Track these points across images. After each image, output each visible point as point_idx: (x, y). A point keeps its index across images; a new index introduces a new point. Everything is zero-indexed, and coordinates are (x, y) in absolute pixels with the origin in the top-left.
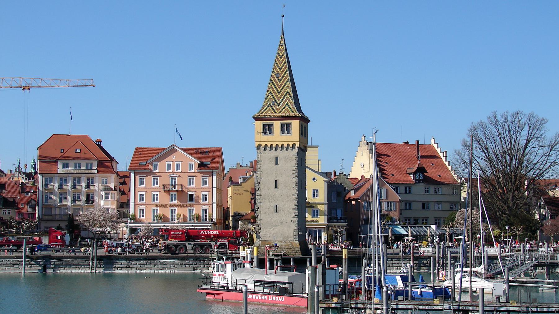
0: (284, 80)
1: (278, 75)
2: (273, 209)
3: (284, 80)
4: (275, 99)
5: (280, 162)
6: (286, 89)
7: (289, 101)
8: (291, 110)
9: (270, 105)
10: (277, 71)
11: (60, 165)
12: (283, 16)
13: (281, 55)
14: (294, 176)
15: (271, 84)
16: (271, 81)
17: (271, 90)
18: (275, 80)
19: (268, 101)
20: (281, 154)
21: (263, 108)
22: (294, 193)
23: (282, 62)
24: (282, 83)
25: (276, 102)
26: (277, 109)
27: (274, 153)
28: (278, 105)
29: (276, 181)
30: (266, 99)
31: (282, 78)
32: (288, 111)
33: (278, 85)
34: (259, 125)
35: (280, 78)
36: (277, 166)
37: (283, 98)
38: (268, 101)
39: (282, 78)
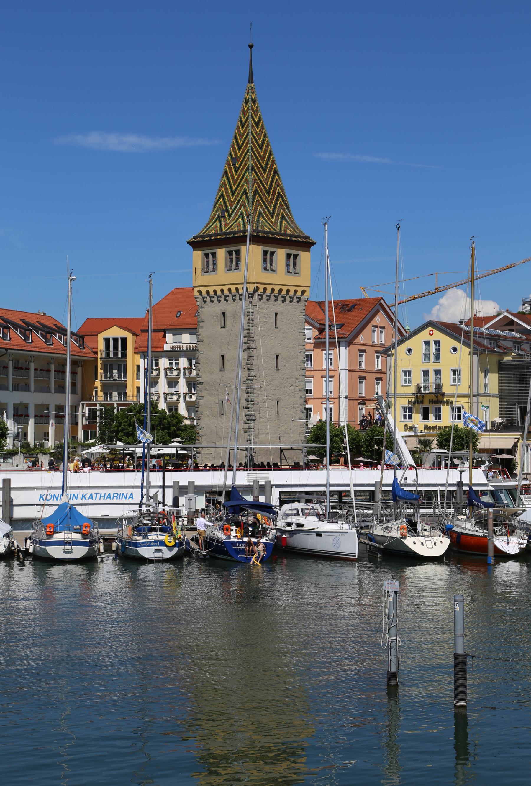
0: (243, 169)
1: (234, 160)
3: (243, 169)
6: (243, 186)
9: (218, 217)
10: (236, 154)
11: (169, 338)
12: (251, 47)
13: (244, 120)
14: (246, 346)
15: (225, 178)
16: (226, 173)
17: (223, 189)
19: (218, 210)
20: (230, 307)
21: (209, 224)
22: (245, 379)
25: (227, 210)
27: (217, 308)
28: (229, 216)
29: (223, 356)
30: (214, 208)
34: (198, 256)
35: (237, 166)
37: (238, 203)
38: (218, 210)
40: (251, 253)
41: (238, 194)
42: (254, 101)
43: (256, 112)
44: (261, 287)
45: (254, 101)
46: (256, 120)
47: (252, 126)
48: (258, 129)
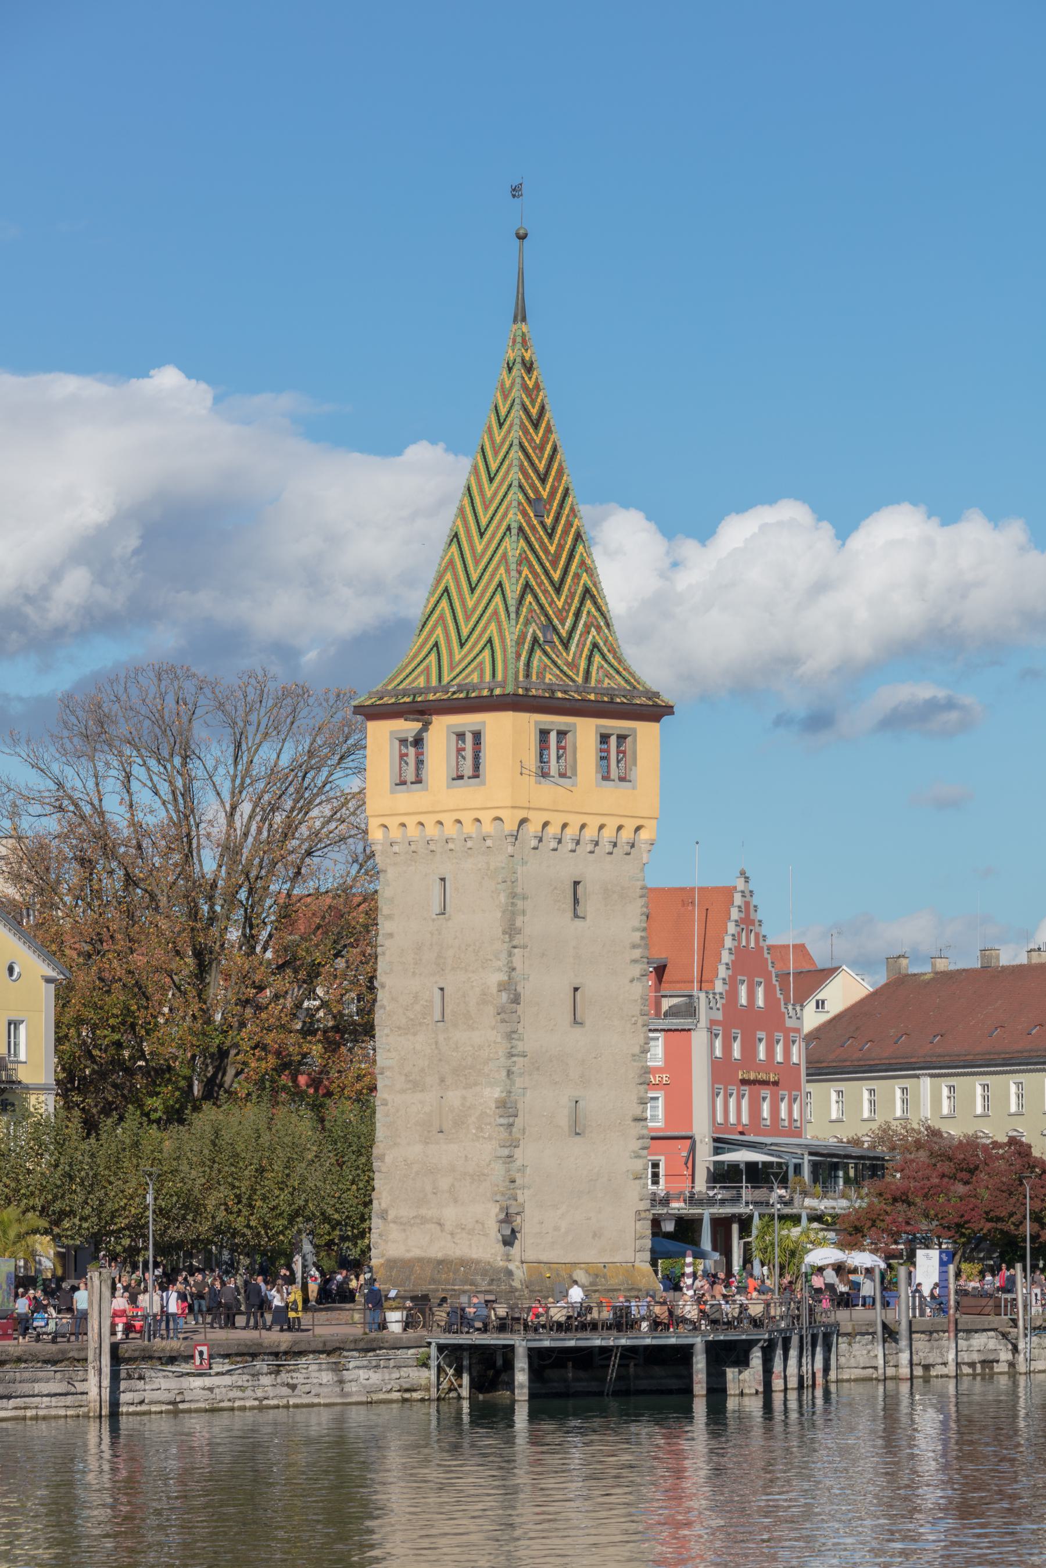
0: (566, 532)
2: (563, 1120)
4: (546, 615)
5: (590, 906)
6: (577, 576)
7: (599, 629)
8: (618, 672)
9: (535, 640)
10: (536, 491)
18: (533, 528)
19: (527, 623)
23: (542, 448)
24: (560, 547)
26: (568, 664)
28: (566, 646)
31: (557, 519)
32: (608, 676)
33: (546, 551)
35: (549, 521)
36: (578, 923)
38: (527, 623)
39: (557, 519)
40: (507, 734)
41: (572, 595)
42: (529, 368)
43: (532, 392)
44: (537, 819)
45: (529, 368)
46: (534, 412)
47: (522, 426)
48: (537, 434)
